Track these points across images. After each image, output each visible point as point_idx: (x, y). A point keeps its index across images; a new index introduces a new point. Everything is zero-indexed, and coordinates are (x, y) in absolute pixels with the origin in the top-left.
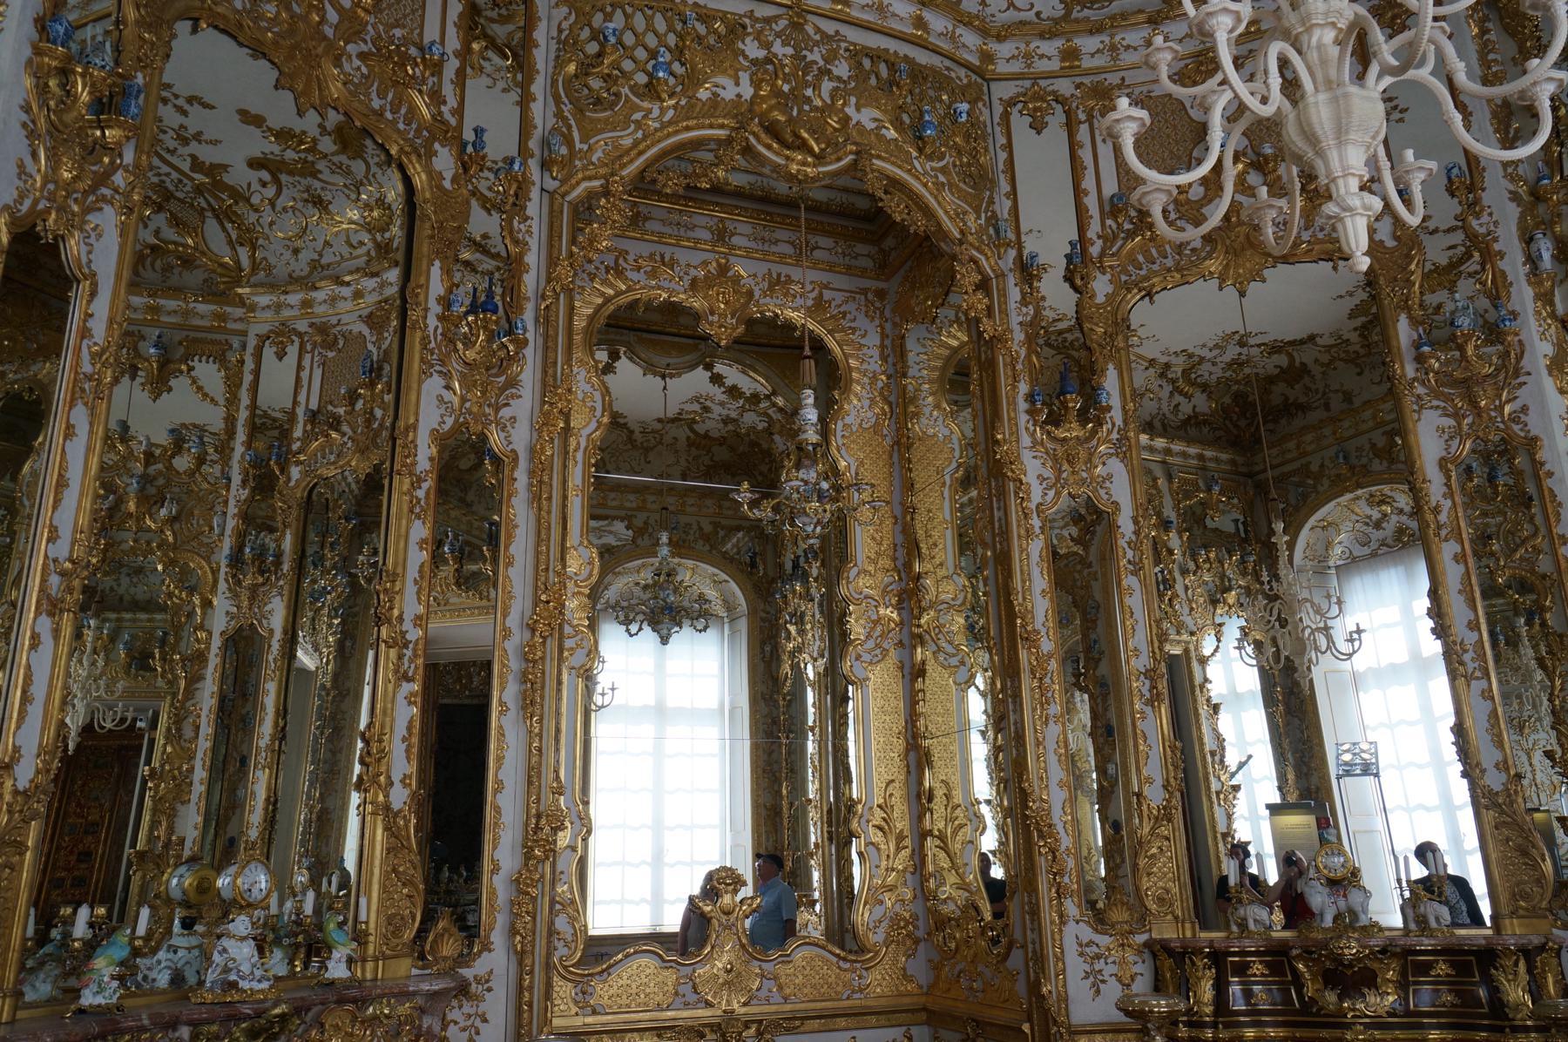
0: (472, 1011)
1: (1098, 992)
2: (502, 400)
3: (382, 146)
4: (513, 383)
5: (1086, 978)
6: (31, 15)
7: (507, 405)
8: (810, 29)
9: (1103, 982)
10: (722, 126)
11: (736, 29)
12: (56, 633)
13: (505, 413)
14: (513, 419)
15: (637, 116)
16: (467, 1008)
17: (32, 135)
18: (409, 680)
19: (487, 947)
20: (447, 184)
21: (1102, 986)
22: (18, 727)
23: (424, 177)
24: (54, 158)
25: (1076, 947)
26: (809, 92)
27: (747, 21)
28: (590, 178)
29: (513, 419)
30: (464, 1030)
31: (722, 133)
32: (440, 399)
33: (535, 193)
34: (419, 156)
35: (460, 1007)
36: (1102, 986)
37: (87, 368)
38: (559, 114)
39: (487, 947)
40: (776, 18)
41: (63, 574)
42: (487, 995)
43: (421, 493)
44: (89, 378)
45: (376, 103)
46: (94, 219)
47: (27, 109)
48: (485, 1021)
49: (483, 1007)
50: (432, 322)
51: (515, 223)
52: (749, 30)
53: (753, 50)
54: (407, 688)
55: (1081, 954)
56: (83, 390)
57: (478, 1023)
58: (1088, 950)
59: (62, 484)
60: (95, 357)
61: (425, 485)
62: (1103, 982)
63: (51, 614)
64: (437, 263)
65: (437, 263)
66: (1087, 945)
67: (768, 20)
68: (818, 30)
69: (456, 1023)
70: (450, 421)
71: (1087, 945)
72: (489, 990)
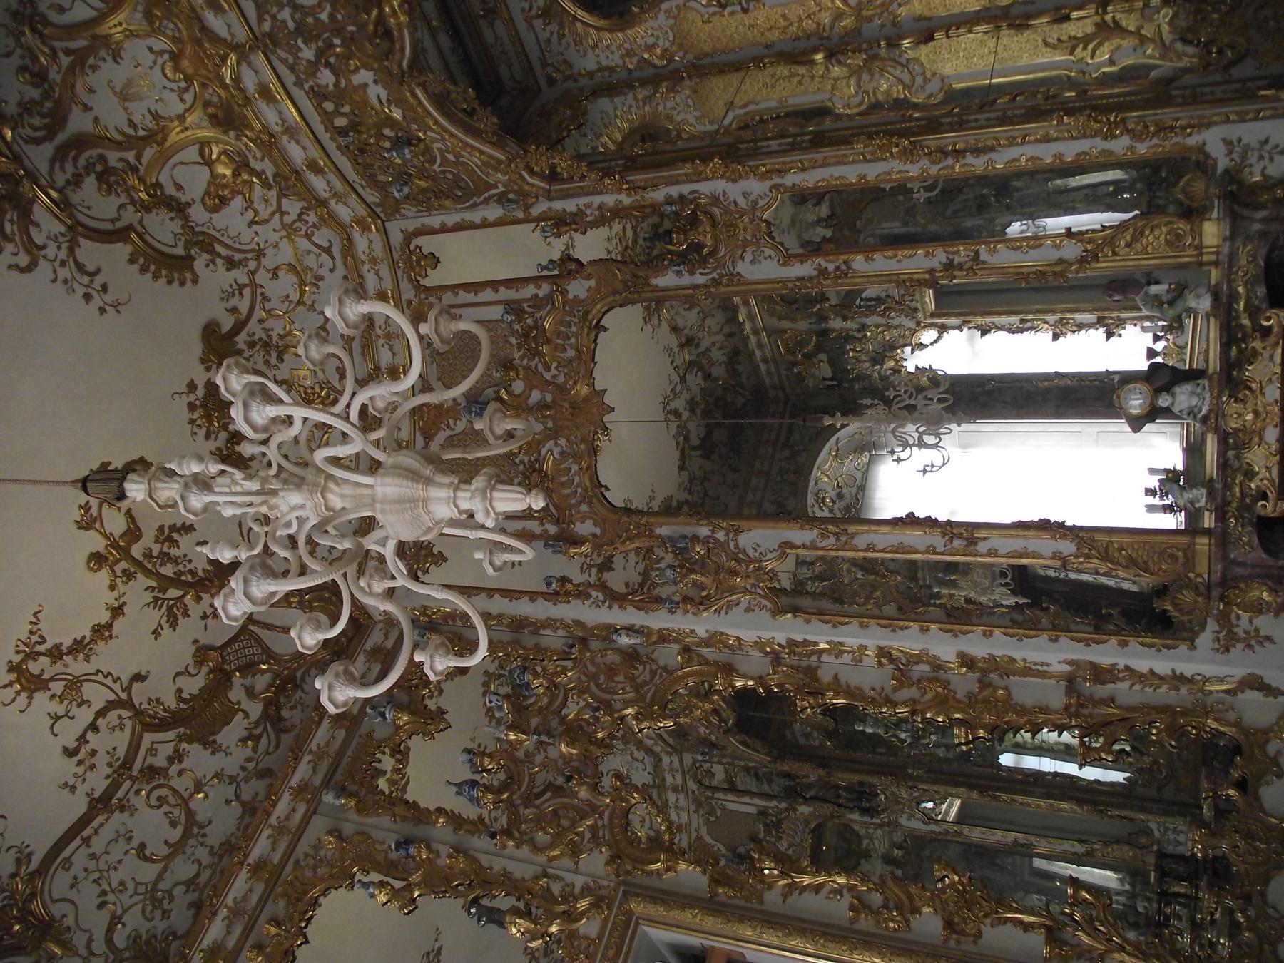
0: (1256, 154)
2: (732, 207)
3: (595, 341)
4: (715, 200)
6: (670, 617)
7: (735, 202)
8: (267, 26)
10: (414, 95)
11: (319, 95)
12: (985, 539)
13: (742, 203)
14: (745, 195)
15: (451, 157)
16: (1253, 158)
17: (729, 606)
18: (977, 253)
19: (1201, 148)
20: (592, 283)
22: (1041, 557)
23: (598, 306)
24: (732, 590)
26: (324, 16)
27: (306, 86)
28: (523, 179)
29: (745, 195)
30: (1271, 159)
31: (419, 92)
32: (753, 262)
33: (558, 205)
34: (587, 313)
35: (1251, 166)
37: (832, 540)
38: (486, 201)
39: (1201, 148)
40: (284, 61)
41: (951, 540)
42: (1244, 141)
43: (831, 267)
44: (838, 539)
45: (571, 353)
46: (751, 552)
47: (718, 612)
48: (1266, 141)
49: (1255, 144)
50: (699, 279)
51: (589, 219)
52: (311, 83)
53: (326, 78)
54: (984, 256)
56: (846, 543)
57: (1268, 147)
59: (900, 548)
60: (823, 536)
61: (824, 264)
63: (975, 544)
64: (654, 281)
65: (654, 281)
67: (292, 69)
68: (260, 19)
69: (1265, 168)
70: (768, 252)
72: (1240, 140)
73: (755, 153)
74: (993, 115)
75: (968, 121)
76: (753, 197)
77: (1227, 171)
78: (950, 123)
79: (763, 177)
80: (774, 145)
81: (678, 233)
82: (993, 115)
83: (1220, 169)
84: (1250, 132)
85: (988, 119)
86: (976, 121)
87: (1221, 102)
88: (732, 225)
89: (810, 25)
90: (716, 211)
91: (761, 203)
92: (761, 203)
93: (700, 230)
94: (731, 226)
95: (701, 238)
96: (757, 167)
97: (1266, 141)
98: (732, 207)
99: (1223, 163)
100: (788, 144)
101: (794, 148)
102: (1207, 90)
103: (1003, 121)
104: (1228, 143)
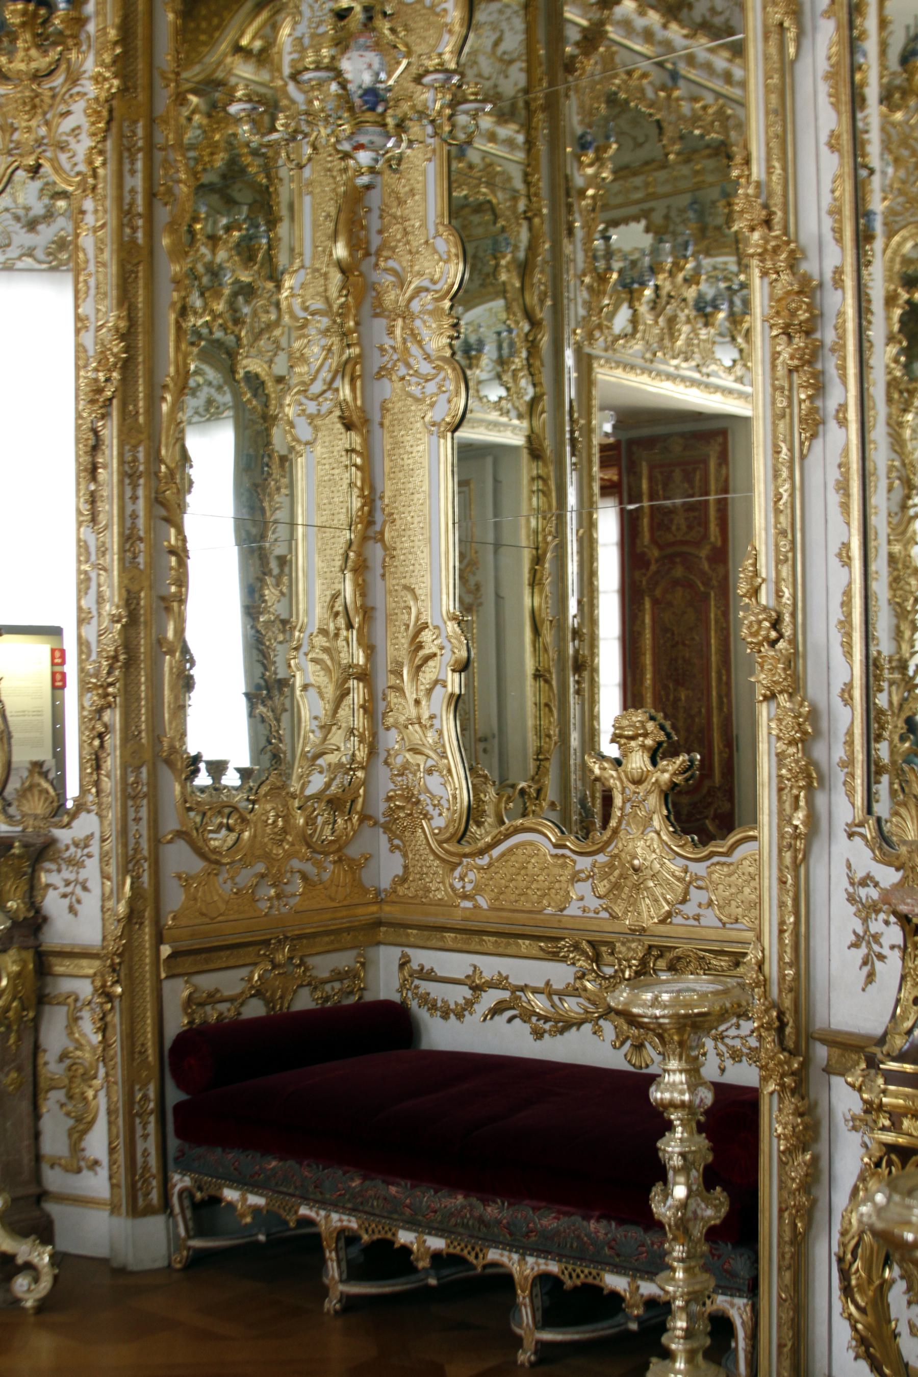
0: (72, 877)
1: (871, 977)
4: (74, 78)
5: (855, 945)
9: (881, 957)
13: (67, 124)
16: (68, 874)
21: (878, 965)
25: (845, 883)
29: (75, 131)
30: (64, 896)
35: (59, 871)
36: (878, 965)
48: (85, 889)
55: (851, 899)
57: (78, 890)
58: (863, 892)
62: (881, 957)
66: (863, 883)
69: (56, 889)
71: (863, 883)
73: (125, 151)
74: (141, 522)
75: (135, 487)
76: (73, 145)
77: (51, 842)
78: (135, 460)
79: (90, 162)
80: (137, 182)
81: (25, 13)
82: (141, 522)
83: (58, 833)
84: (91, 870)
85: (134, 516)
86: (134, 498)
87: (124, 831)
88: (34, 107)
89: (395, 230)
90: (59, 80)
91: (63, 157)
92: (63, 157)
93: (33, 52)
94: (33, 105)
95: (21, 54)
96: (101, 153)
97: (85, 889)
98: (63, 108)
99: (63, 836)
100: (132, 204)
101: (125, 214)
102: (144, 813)
103: (128, 538)
104: (85, 843)
